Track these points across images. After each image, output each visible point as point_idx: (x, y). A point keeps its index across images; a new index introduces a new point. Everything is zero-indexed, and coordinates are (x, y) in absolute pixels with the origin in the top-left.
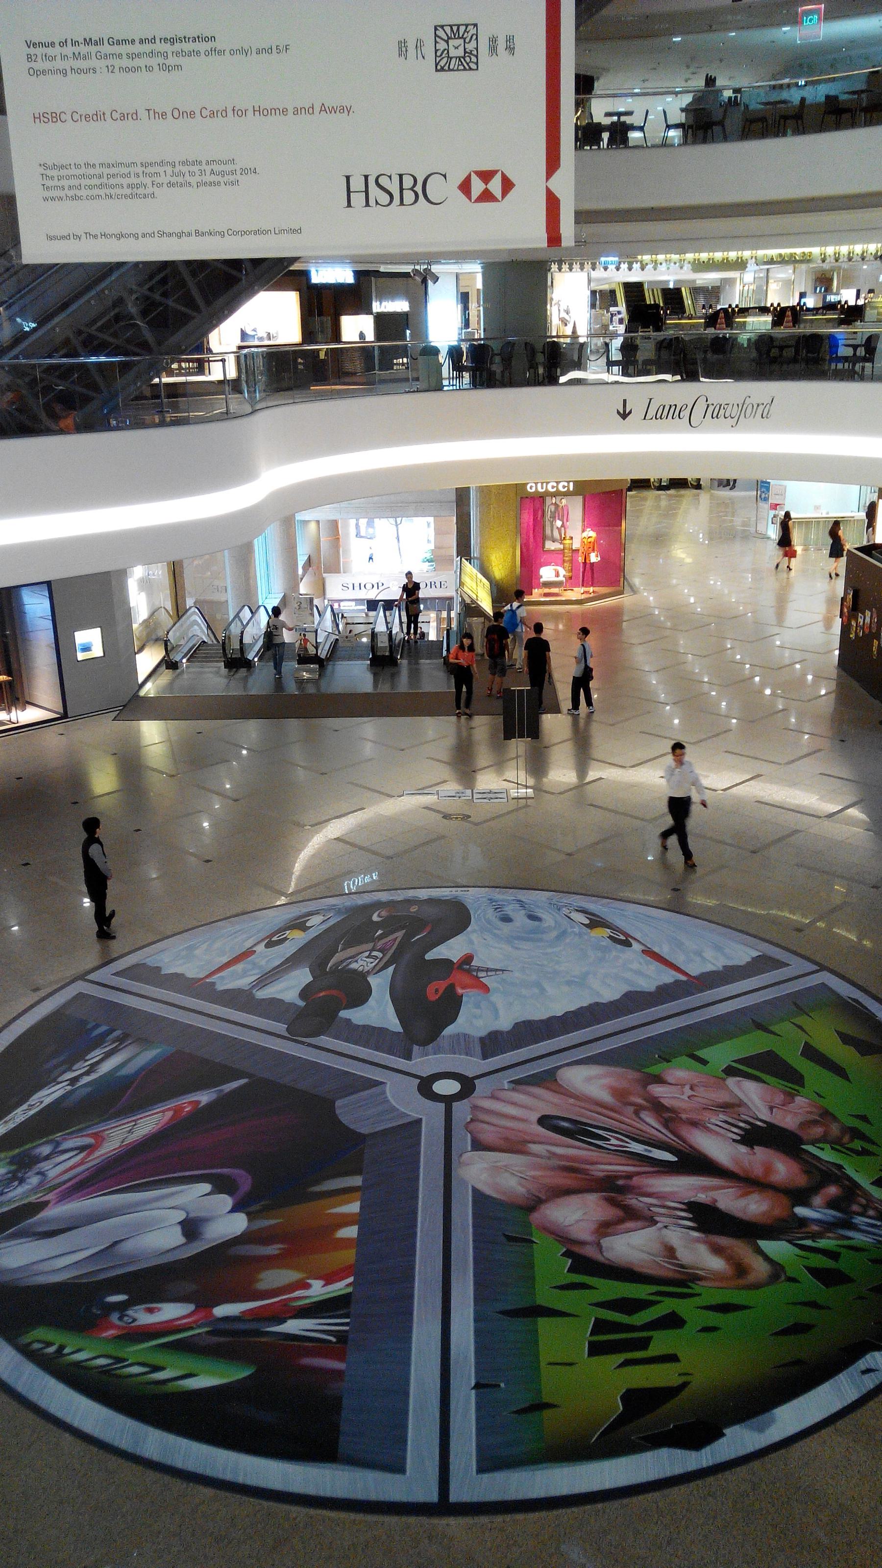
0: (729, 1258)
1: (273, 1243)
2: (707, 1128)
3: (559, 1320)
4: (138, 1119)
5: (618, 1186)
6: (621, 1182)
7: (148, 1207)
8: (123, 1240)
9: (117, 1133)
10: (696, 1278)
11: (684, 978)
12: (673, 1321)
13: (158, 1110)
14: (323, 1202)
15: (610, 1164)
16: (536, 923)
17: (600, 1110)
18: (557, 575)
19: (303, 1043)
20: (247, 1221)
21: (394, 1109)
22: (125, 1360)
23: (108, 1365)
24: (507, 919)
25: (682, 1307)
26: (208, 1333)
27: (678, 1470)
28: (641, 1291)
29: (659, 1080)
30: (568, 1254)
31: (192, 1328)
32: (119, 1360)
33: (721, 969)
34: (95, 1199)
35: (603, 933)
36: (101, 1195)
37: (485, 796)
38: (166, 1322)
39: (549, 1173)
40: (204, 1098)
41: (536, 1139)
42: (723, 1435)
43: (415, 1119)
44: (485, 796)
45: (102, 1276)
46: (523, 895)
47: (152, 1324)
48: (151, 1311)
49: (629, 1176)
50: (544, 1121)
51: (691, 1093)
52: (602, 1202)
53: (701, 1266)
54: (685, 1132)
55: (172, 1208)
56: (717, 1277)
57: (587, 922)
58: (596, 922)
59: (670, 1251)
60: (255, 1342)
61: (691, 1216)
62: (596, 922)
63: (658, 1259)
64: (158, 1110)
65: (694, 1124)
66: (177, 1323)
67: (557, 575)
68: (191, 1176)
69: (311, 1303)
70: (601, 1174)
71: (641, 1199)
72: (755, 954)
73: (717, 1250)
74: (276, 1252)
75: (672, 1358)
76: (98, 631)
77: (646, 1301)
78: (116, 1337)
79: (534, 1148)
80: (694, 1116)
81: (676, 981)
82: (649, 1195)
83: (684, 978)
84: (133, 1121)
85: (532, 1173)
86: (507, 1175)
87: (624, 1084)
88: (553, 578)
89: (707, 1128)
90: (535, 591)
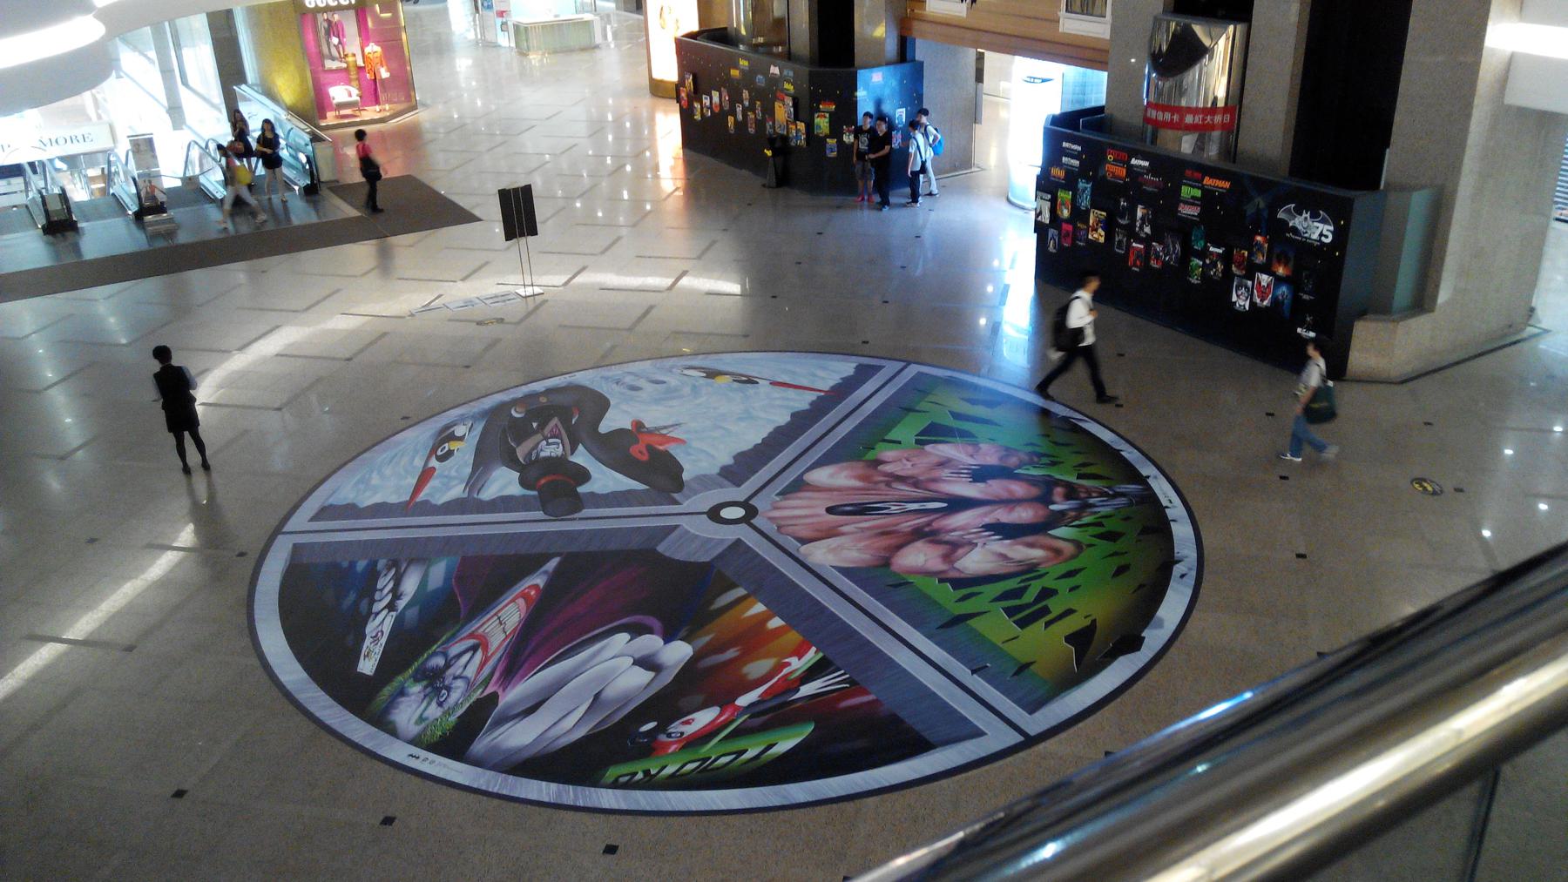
0: (1042, 547)
1: (728, 649)
2: (945, 481)
3: (984, 616)
4: (499, 611)
5: (926, 532)
6: (927, 529)
7: (592, 664)
8: (603, 689)
9: (492, 626)
10: (1037, 565)
11: (822, 394)
12: (1047, 593)
13: (506, 601)
14: (738, 608)
15: (907, 522)
16: (664, 385)
17: (857, 492)
18: (350, 95)
19: (575, 519)
20: (687, 644)
21: (709, 540)
22: (710, 758)
23: (698, 767)
24: (634, 388)
25: (1048, 582)
26: (749, 717)
27: (1135, 669)
28: (1012, 584)
29: (878, 462)
30: (941, 581)
31: (733, 721)
32: (705, 760)
33: (840, 381)
34: (535, 676)
35: (721, 380)
36: (535, 674)
37: (496, 300)
38: (709, 724)
39: (875, 540)
40: (539, 580)
41: (841, 523)
42: (1144, 638)
43: (733, 541)
44: (496, 300)
45: (617, 718)
46: (616, 371)
47: (699, 730)
48: (688, 723)
49: (929, 524)
50: (830, 510)
51: (911, 463)
52: (928, 545)
53: (1030, 557)
54: (933, 486)
55: (612, 658)
56: (1047, 560)
57: (705, 375)
58: (712, 374)
59: (1004, 557)
60: (792, 709)
61: (993, 533)
62: (712, 374)
63: (1001, 563)
64: (506, 601)
65: (935, 480)
66: (719, 721)
67: (350, 95)
68: (590, 638)
69: (804, 672)
70: (909, 529)
71: (953, 534)
72: (855, 365)
73: (1031, 545)
74: (737, 654)
75: (1069, 612)
76: (1278, 216)
77: (1020, 588)
78: (681, 749)
79: (845, 529)
80: (927, 476)
81: (819, 397)
82: (954, 530)
83: (822, 394)
84: (495, 614)
85: (863, 544)
86: (845, 551)
87: (861, 472)
88: (344, 98)
89: (945, 481)
90: (330, 115)
